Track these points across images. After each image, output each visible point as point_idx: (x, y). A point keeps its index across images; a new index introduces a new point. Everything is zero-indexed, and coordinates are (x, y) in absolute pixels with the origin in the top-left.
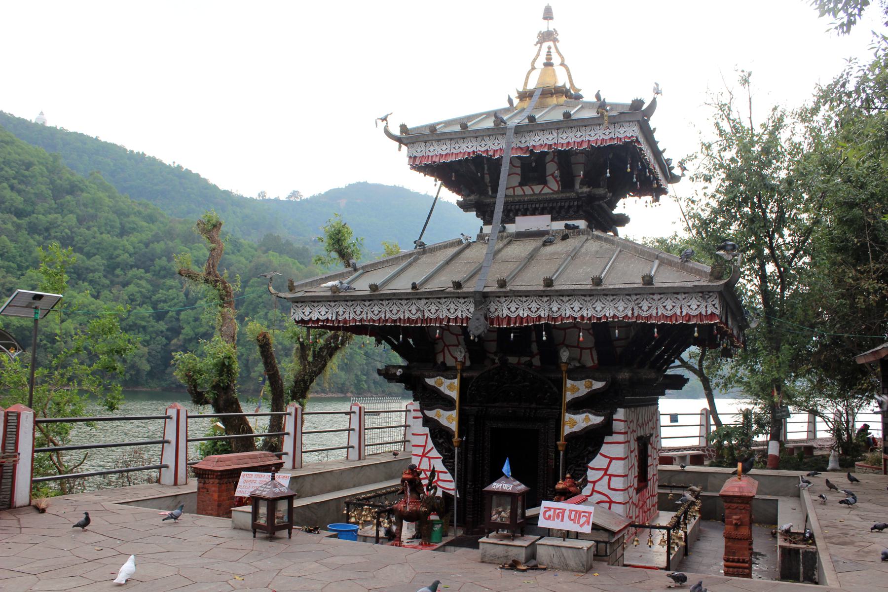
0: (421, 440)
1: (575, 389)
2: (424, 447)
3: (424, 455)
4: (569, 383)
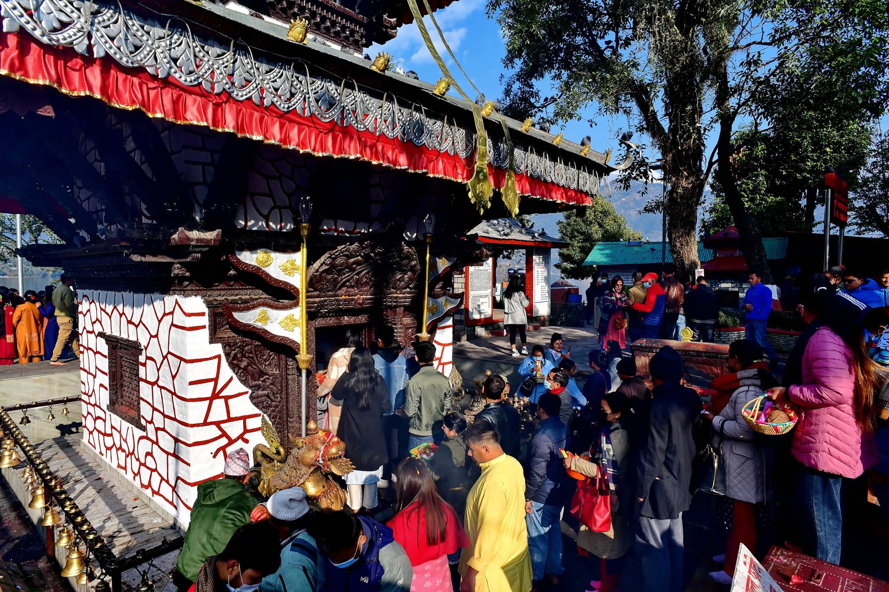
0: (207, 370)
2: (216, 380)
3: (215, 396)
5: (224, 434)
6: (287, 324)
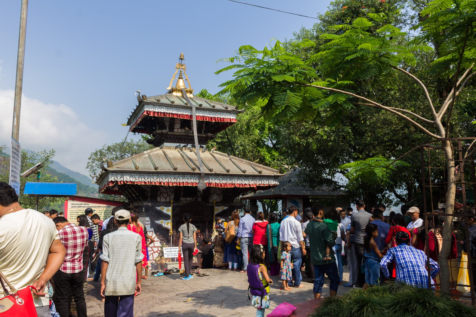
1: (218, 210)
4: (216, 207)
5: (153, 250)
6: (168, 224)
